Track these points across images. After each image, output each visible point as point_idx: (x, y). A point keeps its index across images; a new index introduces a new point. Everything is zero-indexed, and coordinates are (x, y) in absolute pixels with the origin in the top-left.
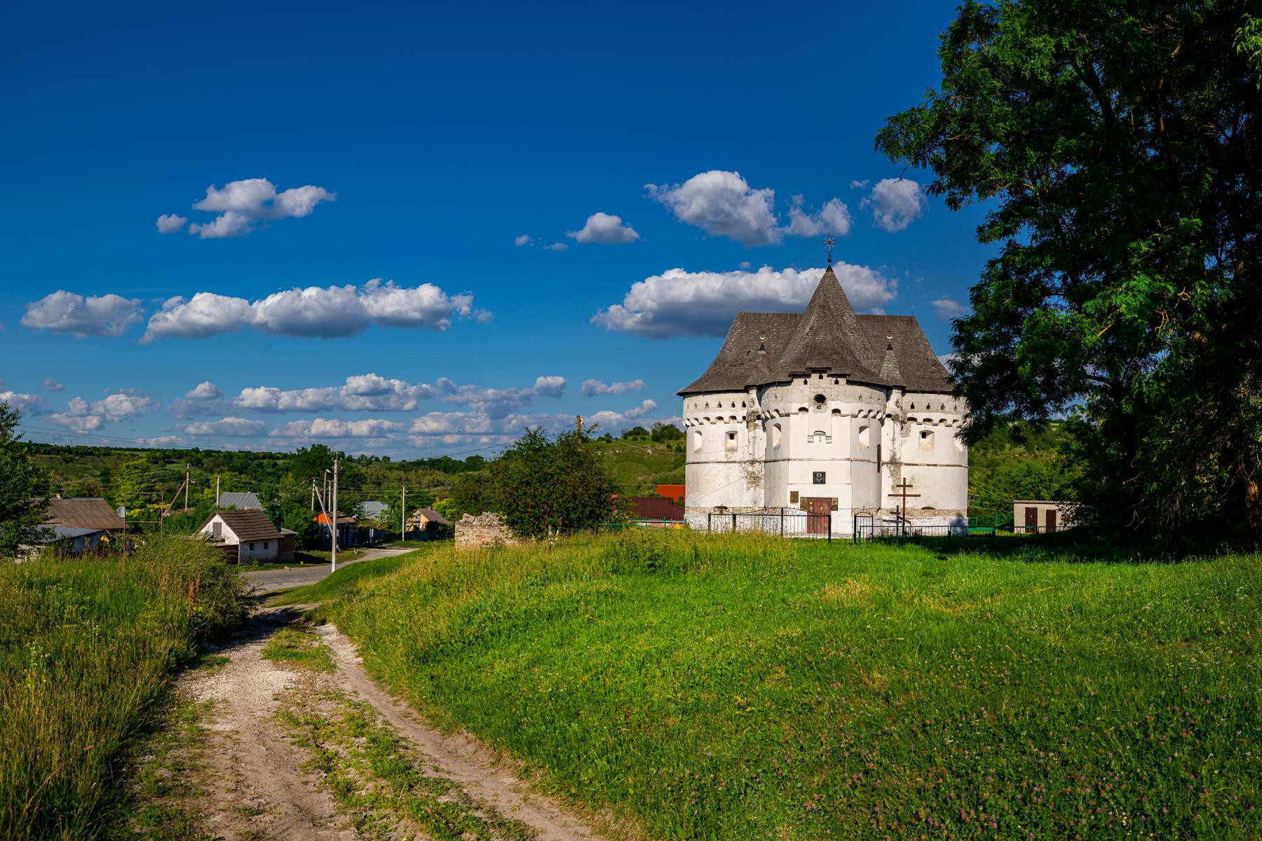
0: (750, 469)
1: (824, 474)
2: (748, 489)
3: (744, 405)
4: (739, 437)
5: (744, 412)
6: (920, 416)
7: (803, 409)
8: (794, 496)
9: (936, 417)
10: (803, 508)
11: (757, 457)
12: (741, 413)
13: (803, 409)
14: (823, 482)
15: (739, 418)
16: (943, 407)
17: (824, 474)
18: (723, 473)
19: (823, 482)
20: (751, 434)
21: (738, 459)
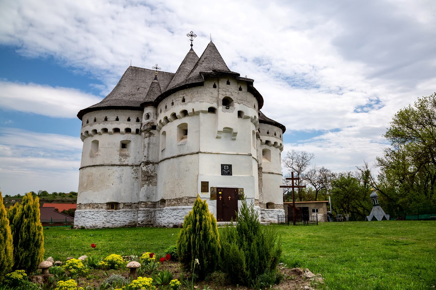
0: (144, 169)
1: (230, 166)
2: (143, 186)
3: (138, 120)
4: (132, 146)
5: (138, 126)
6: (264, 138)
7: (212, 110)
8: (205, 186)
9: (273, 140)
10: (212, 198)
11: (150, 159)
12: (134, 126)
13: (212, 110)
14: (230, 174)
15: (133, 130)
16: (275, 134)
17: (230, 166)
18: (117, 174)
19: (230, 174)
20: (147, 140)
21: (130, 163)
